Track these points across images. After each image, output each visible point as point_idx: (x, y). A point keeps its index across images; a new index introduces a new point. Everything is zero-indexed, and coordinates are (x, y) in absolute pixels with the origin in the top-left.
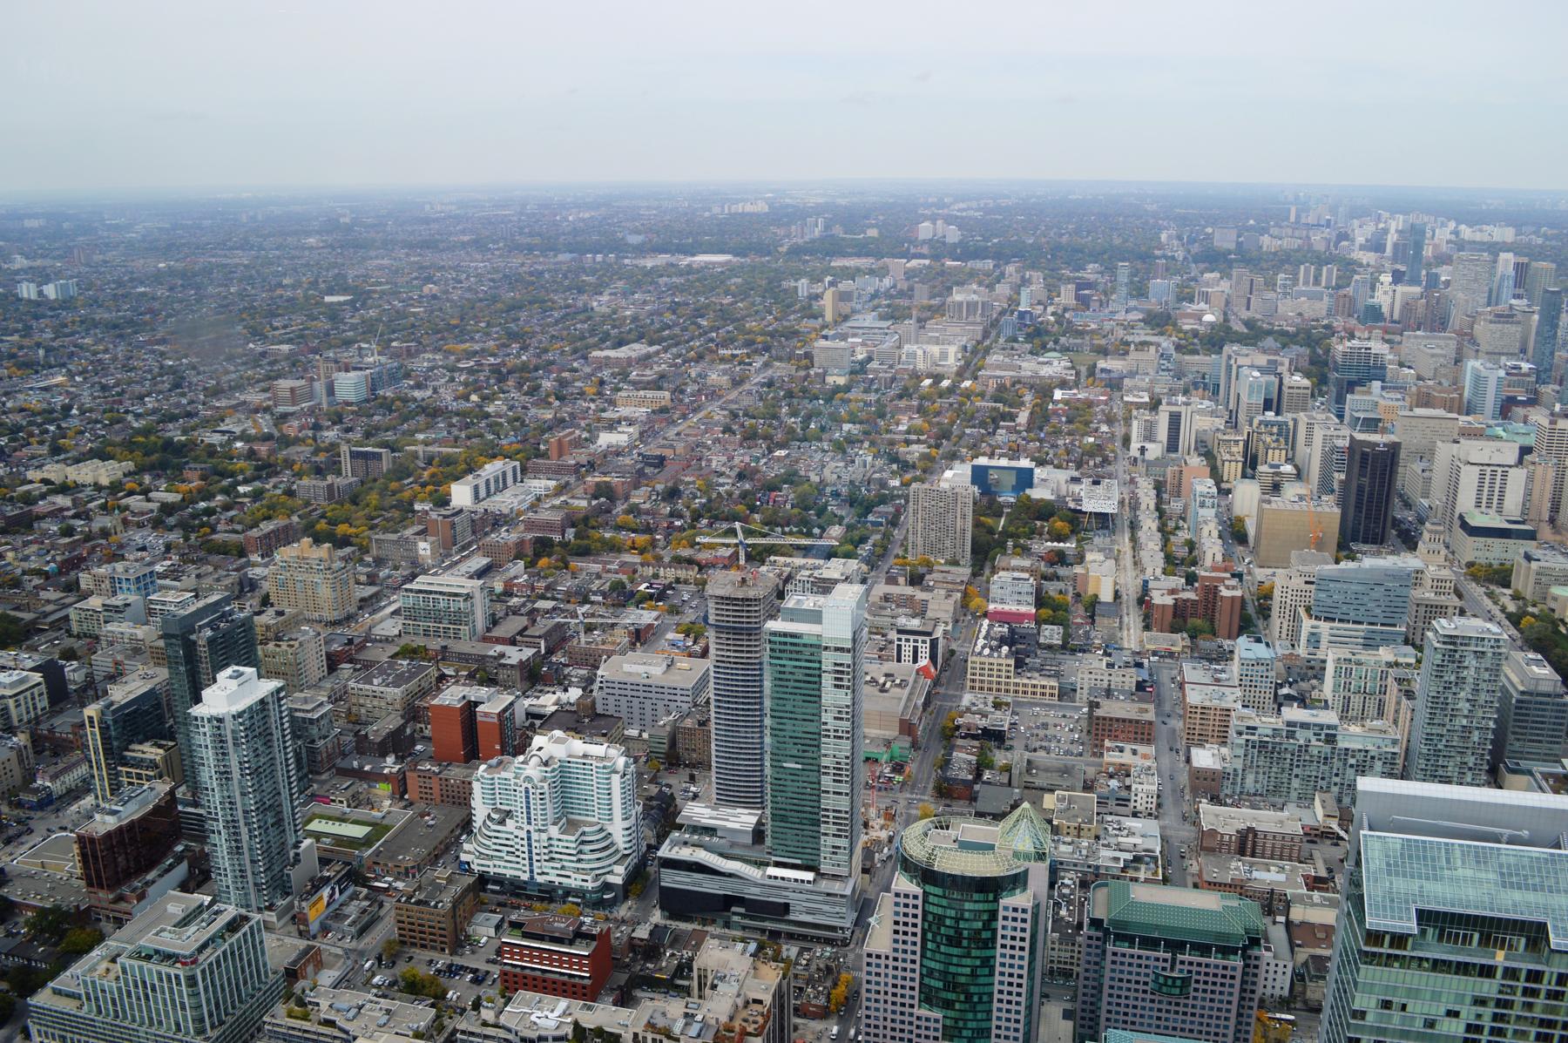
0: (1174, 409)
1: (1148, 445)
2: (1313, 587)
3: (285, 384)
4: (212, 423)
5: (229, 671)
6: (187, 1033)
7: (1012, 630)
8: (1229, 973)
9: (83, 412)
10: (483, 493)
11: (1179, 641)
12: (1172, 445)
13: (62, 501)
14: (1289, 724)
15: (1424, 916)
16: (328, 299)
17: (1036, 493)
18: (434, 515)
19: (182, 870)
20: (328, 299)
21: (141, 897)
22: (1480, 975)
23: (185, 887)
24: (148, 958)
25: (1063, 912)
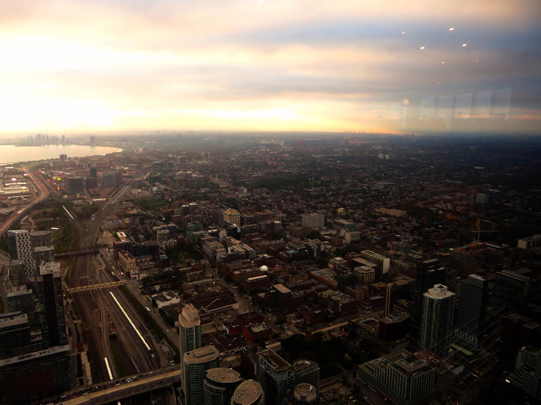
3: (458, 194)
4: (432, 204)
5: (439, 285)
6: (403, 397)
9: (393, 194)
10: (531, 245)
13: (385, 219)
16: (476, 168)
18: (510, 249)
19: (407, 343)
20: (476, 168)
21: (394, 347)
23: (406, 349)
24: (397, 368)
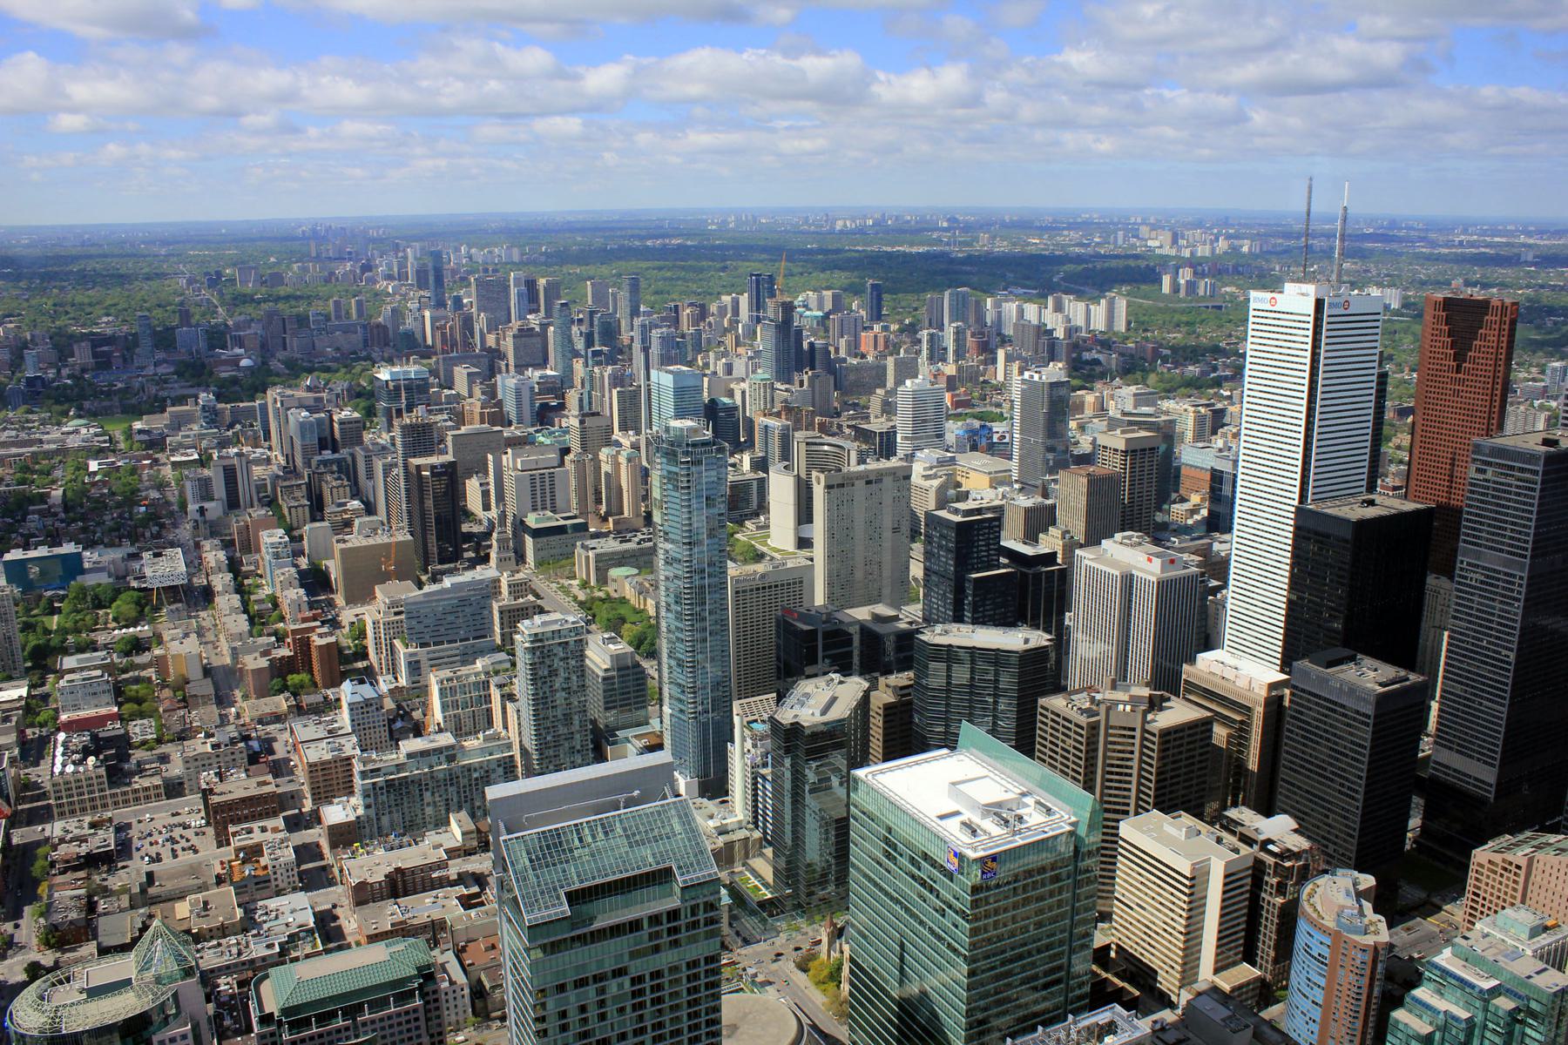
0: (227, 462)
1: (206, 505)
2: (403, 616)
7: (94, 738)
8: (412, 1016)
11: (282, 702)
12: (233, 503)
14: (410, 756)
15: (573, 897)
17: (90, 580)
22: (631, 931)
25: (227, 1022)
